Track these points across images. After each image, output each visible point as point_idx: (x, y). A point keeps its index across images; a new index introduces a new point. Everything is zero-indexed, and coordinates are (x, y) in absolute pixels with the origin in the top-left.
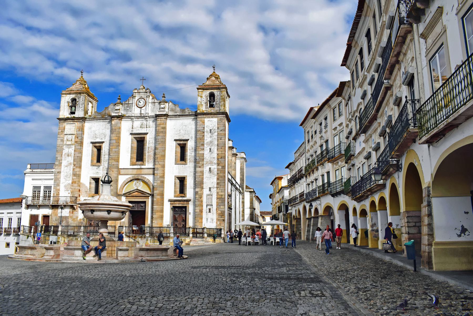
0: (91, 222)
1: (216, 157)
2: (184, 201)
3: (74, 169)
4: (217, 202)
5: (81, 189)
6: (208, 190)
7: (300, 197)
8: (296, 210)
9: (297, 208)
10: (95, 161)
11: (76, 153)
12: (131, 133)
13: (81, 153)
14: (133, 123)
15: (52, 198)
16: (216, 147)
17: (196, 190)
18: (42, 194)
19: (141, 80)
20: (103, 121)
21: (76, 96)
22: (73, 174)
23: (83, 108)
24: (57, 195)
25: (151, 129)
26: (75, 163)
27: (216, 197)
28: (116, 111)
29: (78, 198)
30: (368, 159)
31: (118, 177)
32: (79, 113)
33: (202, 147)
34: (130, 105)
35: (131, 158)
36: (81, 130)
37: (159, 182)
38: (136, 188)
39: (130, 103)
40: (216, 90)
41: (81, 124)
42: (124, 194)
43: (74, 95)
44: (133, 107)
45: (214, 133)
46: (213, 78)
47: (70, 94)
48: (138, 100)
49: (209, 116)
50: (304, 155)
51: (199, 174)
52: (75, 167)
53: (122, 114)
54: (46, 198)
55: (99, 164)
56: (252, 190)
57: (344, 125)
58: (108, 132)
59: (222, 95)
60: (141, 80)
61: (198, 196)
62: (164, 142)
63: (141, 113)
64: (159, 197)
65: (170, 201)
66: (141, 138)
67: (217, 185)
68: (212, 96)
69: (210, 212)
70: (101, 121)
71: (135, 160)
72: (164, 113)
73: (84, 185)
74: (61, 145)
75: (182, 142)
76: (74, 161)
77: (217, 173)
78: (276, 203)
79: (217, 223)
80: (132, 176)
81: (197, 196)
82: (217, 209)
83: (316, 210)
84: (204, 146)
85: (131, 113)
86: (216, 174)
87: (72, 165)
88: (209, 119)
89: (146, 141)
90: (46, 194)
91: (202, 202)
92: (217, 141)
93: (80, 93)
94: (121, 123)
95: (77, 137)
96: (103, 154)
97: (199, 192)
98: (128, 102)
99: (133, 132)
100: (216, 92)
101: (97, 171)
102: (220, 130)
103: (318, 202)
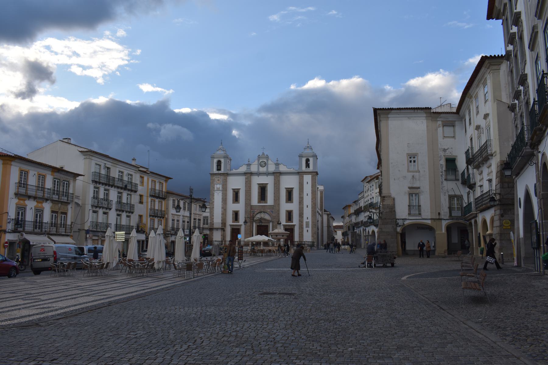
2: (292, 225)
7: (361, 223)
9: (359, 229)
10: (235, 200)
50: (363, 199)
56: (329, 213)
61: (301, 221)
68: (307, 161)
75: (289, 190)
83: (368, 231)
103: (369, 228)
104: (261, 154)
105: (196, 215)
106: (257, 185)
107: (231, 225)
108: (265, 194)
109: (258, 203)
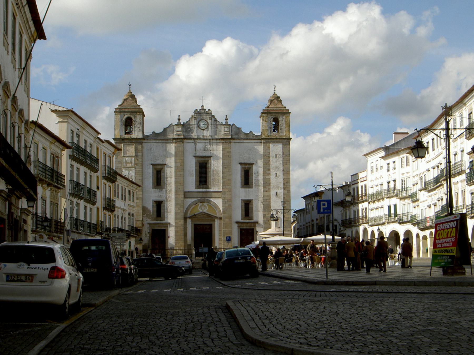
2: (251, 223)
11: (136, 176)
12: (194, 155)
14: (195, 146)
20: (163, 141)
30: (429, 207)
32: (136, 134)
33: (268, 172)
34: (191, 126)
37: (227, 205)
38: (201, 211)
39: (191, 124)
42: (190, 218)
46: (276, 101)
47: (125, 112)
49: (274, 141)
57: (410, 174)
59: (286, 120)
60: (200, 99)
64: (227, 220)
65: (237, 222)
66: (205, 160)
70: (161, 141)
73: (147, 209)
74: (119, 167)
75: (247, 166)
95: (137, 160)
101: (160, 194)
102: (285, 156)
107: (148, 224)
108: (206, 174)
109: (195, 188)
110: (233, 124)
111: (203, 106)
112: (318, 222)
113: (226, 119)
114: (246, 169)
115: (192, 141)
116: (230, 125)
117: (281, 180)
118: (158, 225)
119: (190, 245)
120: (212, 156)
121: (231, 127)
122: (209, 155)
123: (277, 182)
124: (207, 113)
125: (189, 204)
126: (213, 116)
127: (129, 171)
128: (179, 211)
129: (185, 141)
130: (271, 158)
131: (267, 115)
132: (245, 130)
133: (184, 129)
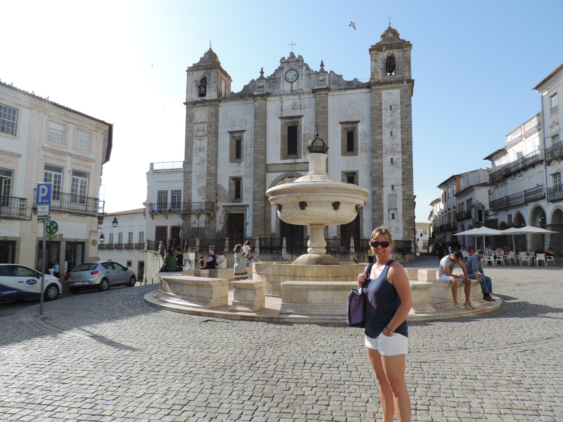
0: (232, 235)
1: (400, 143)
3: (208, 167)
4: (403, 205)
5: (218, 193)
6: (390, 188)
8: (510, 216)
10: (234, 156)
12: (280, 116)
13: (217, 146)
14: (282, 104)
15: (182, 205)
16: (400, 129)
17: (373, 190)
18: (169, 201)
19: (289, 45)
21: (205, 73)
22: (207, 174)
23: (215, 88)
24: (188, 201)
25: (307, 110)
26: (210, 159)
27: (402, 197)
28: (259, 89)
29: (215, 204)
31: (265, 175)
33: (379, 131)
35: (282, 150)
36: (214, 116)
40: (396, 50)
41: (215, 109)
43: (203, 72)
44: (282, 83)
45: (396, 109)
46: (390, 35)
47: (198, 70)
48: (287, 72)
51: (377, 167)
52: (210, 165)
53: (266, 92)
54: (175, 205)
55: (239, 160)
58: (250, 118)
59: (405, 56)
60: (289, 45)
62: (326, 127)
63: (292, 89)
66: (294, 122)
67: (402, 181)
69: (393, 218)
71: (286, 153)
72: (325, 87)
73: (223, 187)
76: (208, 156)
77: (403, 166)
78: (449, 209)
79: (404, 233)
80: (283, 173)
81: (375, 197)
82: (403, 214)
84: (382, 129)
85: (279, 90)
86: (401, 166)
87: (206, 162)
88: (388, 91)
89: (301, 127)
90: (175, 200)
91: (382, 204)
92: (401, 121)
93: (211, 69)
94: (266, 104)
96: (244, 146)
97: (377, 192)
98: (274, 76)
99: (283, 116)
100: (397, 53)
101: (238, 168)
102: (404, 106)
104: (287, 56)
105: (63, 158)
106: (279, 123)
107: (223, 206)
110: (332, 72)
111: (292, 55)
112: (455, 210)
113: (322, 65)
114: (350, 130)
115: (277, 98)
116: (327, 73)
117: (398, 140)
118: (234, 209)
119: (275, 233)
120: (303, 116)
121: (328, 75)
122: (299, 114)
123: (393, 145)
124: (298, 61)
125: (272, 181)
126: (306, 65)
127: (200, 140)
128: (258, 189)
129: (269, 99)
130: (383, 111)
131: (377, 52)
132: (347, 77)
133: (268, 85)
